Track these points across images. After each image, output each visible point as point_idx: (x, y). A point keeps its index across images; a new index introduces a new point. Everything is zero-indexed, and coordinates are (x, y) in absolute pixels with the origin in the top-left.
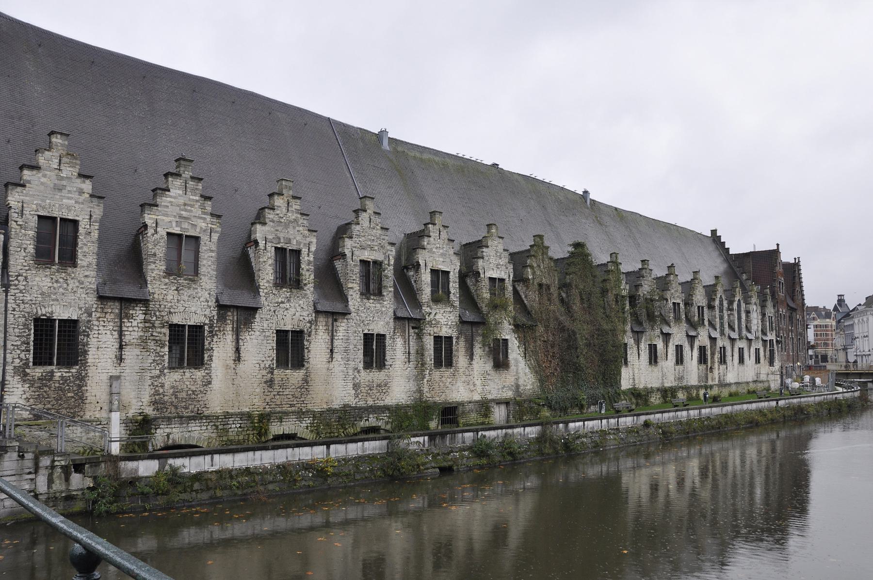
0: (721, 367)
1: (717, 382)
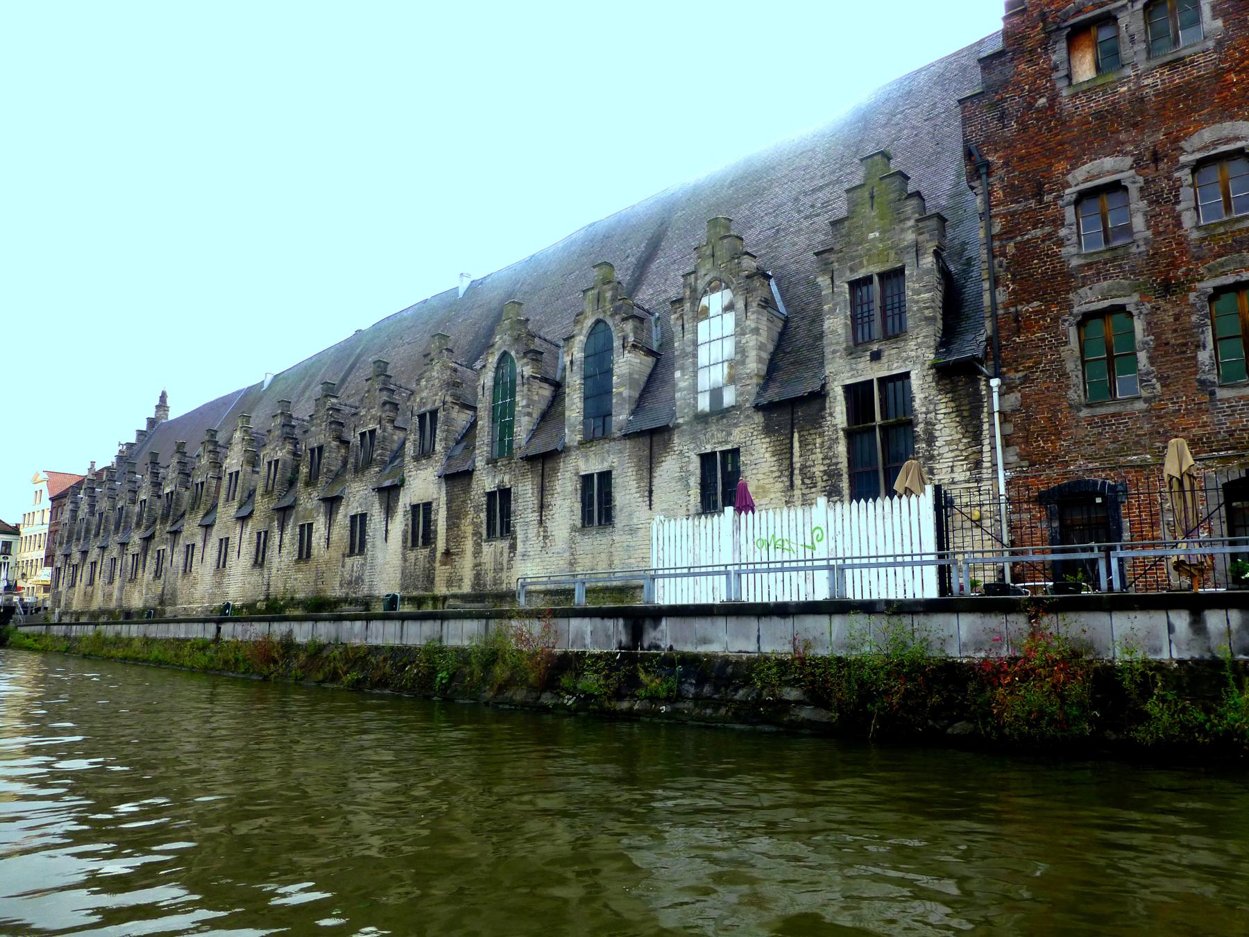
0: (488, 550)
1: (466, 588)
